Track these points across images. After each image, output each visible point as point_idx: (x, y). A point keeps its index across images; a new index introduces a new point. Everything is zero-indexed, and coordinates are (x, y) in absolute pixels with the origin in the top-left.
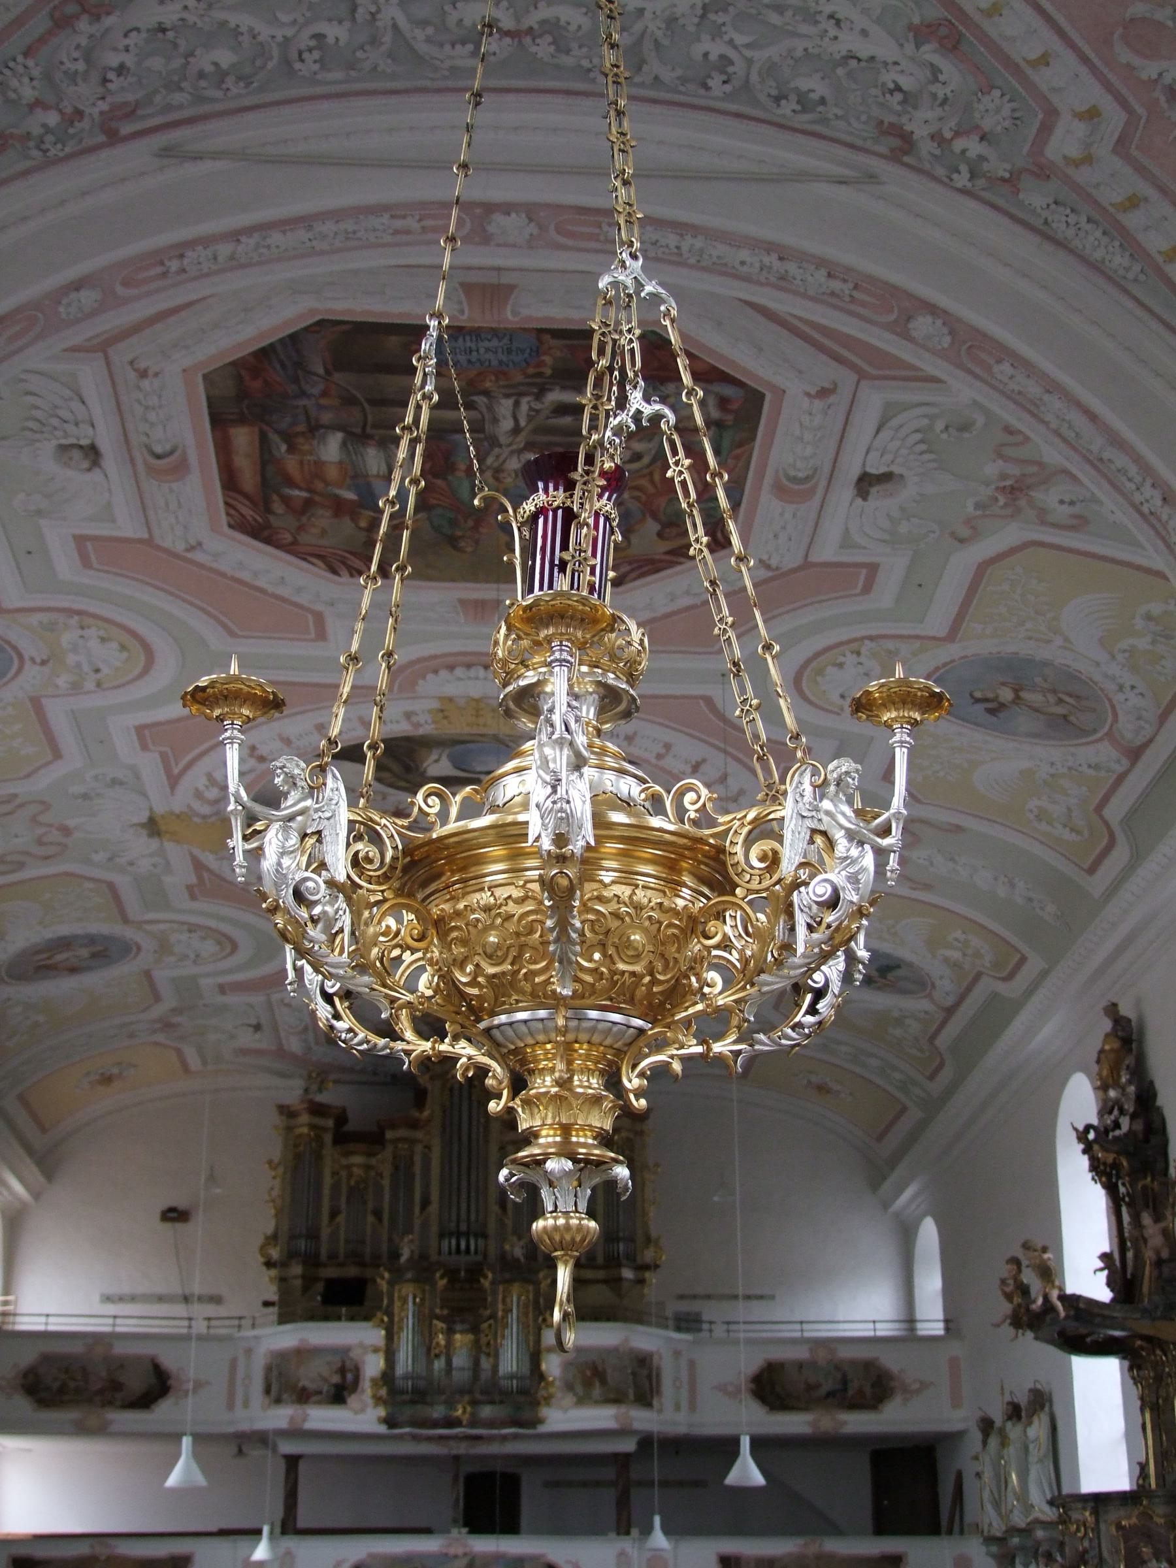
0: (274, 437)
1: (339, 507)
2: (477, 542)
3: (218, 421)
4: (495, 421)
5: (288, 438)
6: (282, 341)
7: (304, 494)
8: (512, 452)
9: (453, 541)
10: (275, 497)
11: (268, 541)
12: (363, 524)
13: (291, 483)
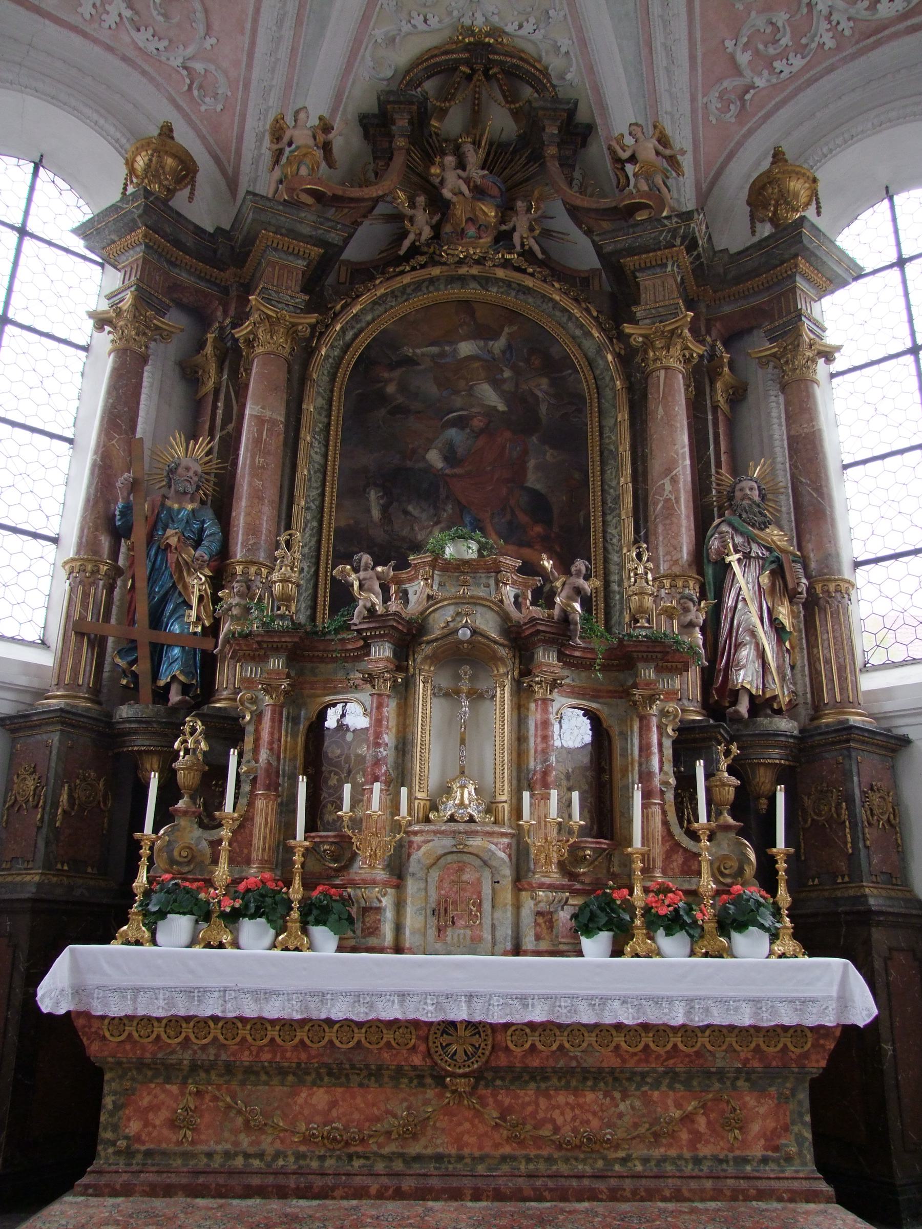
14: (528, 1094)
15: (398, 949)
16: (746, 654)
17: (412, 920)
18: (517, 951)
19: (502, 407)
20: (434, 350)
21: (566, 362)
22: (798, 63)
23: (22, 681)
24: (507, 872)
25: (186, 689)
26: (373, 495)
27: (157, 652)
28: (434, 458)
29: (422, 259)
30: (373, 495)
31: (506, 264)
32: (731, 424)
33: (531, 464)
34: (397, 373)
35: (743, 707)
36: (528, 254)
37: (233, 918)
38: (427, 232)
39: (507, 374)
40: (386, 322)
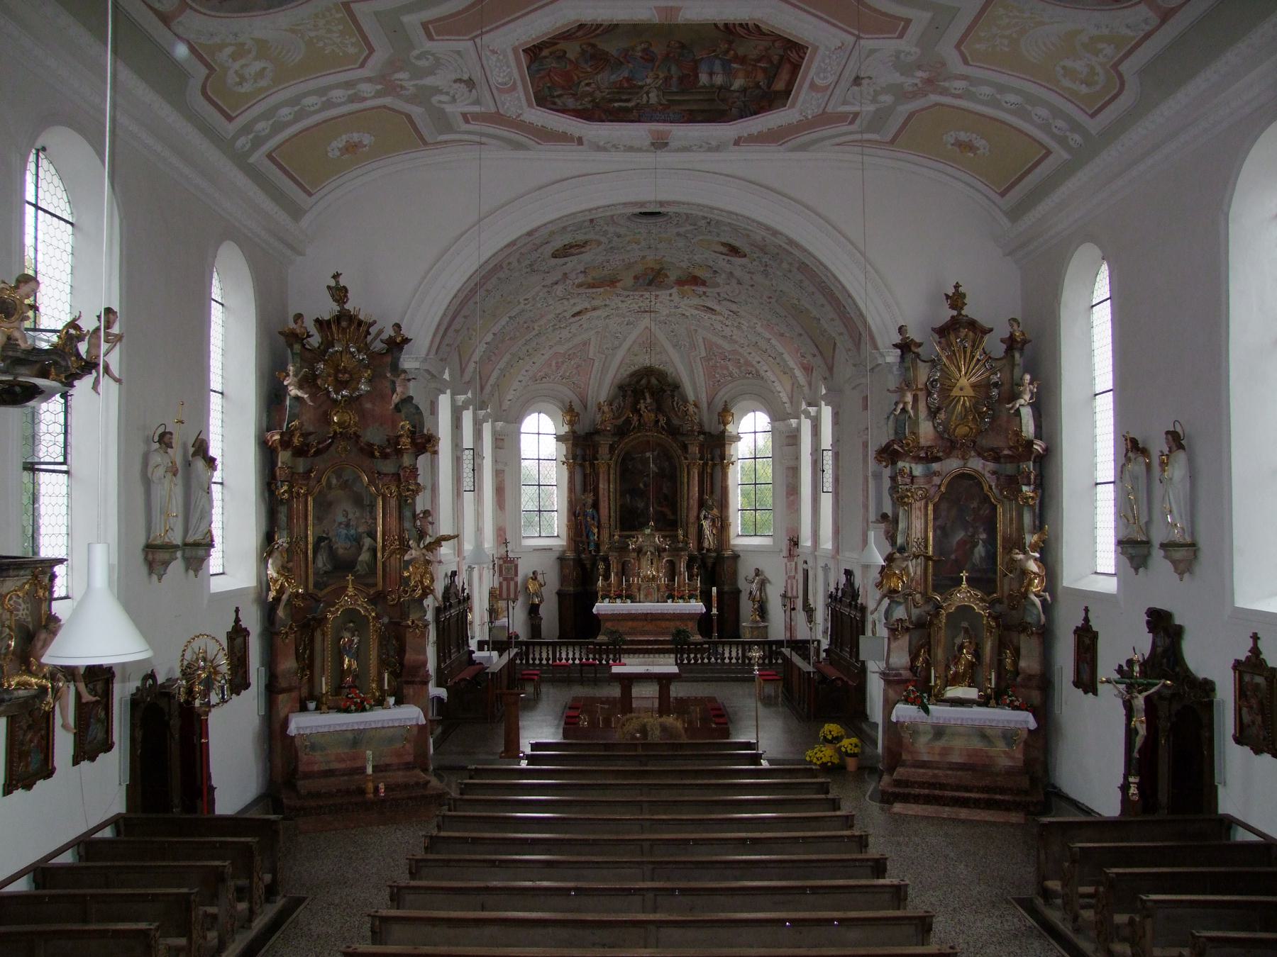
0: (764, 87)
1: (742, 60)
2: (668, 46)
3: (787, 93)
4: (658, 96)
5: (757, 86)
6: (746, 117)
7: (759, 64)
8: (649, 85)
9: (683, 46)
10: (775, 62)
11: (789, 41)
12: (732, 52)
13: (764, 70)
14: (659, 622)
15: (640, 602)
16: (706, 540)
17: (642, 596)
18: (658, 602)
23: (561, 549)
25: (595, 551)
26: (628, 496)
27: (588, 544)
28: (641, 485)
29: (635, 430)
30: (628, 496)
32: (712, 475)
35: (705, 551)
36: (662, 427)
37: (615, 599)
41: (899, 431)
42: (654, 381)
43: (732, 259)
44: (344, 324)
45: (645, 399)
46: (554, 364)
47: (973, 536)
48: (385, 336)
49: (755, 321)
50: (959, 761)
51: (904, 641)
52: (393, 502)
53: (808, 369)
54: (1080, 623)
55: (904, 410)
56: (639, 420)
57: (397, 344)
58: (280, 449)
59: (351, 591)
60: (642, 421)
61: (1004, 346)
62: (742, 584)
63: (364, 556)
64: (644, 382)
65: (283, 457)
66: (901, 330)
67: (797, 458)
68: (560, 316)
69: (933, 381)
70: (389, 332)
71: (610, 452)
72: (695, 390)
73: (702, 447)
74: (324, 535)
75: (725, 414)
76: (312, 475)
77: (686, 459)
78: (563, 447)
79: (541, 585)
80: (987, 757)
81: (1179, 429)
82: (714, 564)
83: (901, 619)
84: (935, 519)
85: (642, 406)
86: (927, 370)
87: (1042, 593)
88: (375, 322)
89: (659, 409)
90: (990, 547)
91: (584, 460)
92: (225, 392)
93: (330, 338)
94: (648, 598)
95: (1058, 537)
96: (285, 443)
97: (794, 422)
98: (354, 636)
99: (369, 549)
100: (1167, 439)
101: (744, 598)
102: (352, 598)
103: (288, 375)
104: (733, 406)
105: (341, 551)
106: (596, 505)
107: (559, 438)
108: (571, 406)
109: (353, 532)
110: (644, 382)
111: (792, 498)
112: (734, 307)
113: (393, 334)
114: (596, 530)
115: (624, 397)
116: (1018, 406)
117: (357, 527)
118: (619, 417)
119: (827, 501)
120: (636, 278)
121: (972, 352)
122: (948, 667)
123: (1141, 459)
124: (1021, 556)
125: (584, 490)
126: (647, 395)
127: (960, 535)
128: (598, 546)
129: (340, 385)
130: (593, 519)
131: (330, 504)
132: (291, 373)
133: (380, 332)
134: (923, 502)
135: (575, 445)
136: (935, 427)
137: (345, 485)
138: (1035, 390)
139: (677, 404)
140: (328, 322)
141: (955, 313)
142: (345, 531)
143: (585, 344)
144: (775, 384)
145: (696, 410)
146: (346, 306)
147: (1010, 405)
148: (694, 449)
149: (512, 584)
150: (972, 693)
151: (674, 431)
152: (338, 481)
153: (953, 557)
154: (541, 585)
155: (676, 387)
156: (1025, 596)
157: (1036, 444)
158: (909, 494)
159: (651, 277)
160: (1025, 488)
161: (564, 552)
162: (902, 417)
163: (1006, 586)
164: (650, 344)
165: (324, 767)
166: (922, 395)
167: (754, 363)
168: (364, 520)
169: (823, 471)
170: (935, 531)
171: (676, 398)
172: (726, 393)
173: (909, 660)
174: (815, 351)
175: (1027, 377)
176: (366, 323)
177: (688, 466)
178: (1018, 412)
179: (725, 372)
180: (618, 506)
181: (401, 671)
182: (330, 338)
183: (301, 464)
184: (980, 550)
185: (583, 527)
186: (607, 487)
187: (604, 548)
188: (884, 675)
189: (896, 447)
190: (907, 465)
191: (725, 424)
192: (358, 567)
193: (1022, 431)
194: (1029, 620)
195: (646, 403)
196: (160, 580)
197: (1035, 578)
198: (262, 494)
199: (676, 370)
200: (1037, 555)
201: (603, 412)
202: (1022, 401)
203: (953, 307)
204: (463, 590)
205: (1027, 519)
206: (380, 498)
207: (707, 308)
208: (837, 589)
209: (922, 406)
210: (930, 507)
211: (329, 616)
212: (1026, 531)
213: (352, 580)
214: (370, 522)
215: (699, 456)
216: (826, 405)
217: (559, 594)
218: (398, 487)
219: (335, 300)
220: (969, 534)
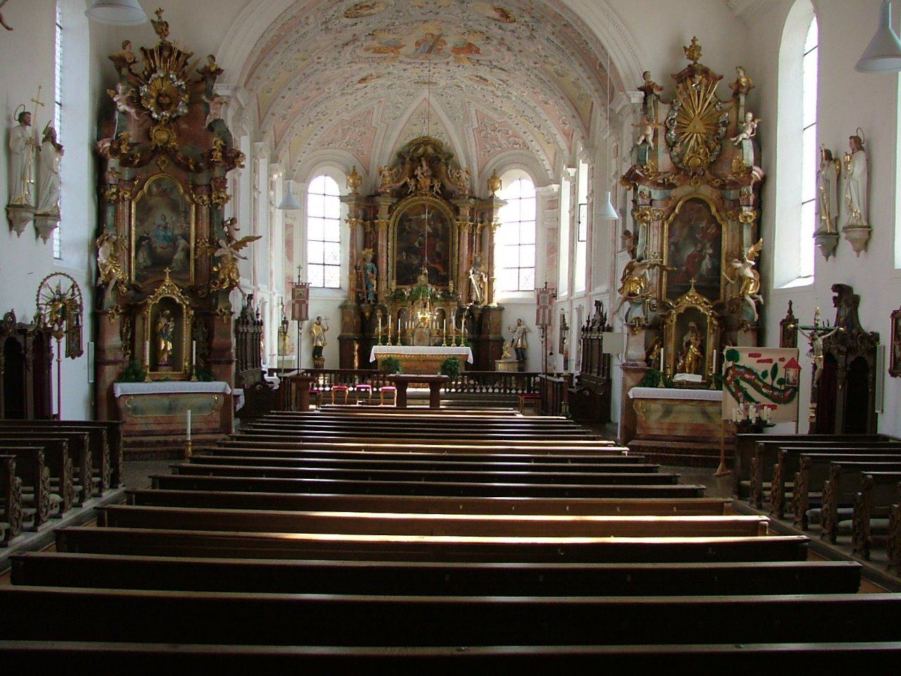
18: (430, 345)
19: (431, 231)
20: (416, 217)
21: (446, 219)
22: (500, 149)
24: (428, 335)
25: (373, 301)
27: (368, 294)
28: (417, 244)
29: (413, 194)
31: (432, 196)
32: (481, 236)
33: (437, 245)
34: (408, 223)
36: (437, 193)
38: (414, 188)
39: (432, 223)
40: (405, 210)
41: (641, 162)
42: (430, 150)
43: (504, 25)
44: (166, 53)
45: (421, 166)
46: (340, 131)
47: (701, 251)
48: (201, 66)
49: (522, 89)
50: (685, 435)
51: (641, 336)
52: (205, 210)
53: (568, 135)
54: (785, 315)
55: (645, 141)
56: (416, 185)
57: (211, 74)
58: (109, 156)
59: (168, 281)
60: (419, 186)
61: (732, 91)
62: (505, 334)
63: (179, 256)
64: (421, 151)
65: (113, 163)
66: (645, 75)
67: (558, 220)
68: (348, 81)
69: (671, 119)
70: (205, 62)
71: (389, 213)
72: (467, 158)
73: (472, 209)
74: (145, 235)
75: (492, 181)
76: (136, 183)
77: (458, 220)
78: (346, 207)
79: (324, 330)
80: (708, 431)
81: (860, 136)
82: (481, 316)
83: (638, 318)
84: (669, 237)
85: (418, 172)
86: (667, 111)
87: (756, 296)
88: (192, 54)
89: (435, 176)
90: (714, 260)
91: (365, 220)
92: (63, 103)
93: (153, 66)
94: (421, 342)
95: (772, 249)
96: (115, 152)
97: (555, 187)
98: (169, 321)
99: (183, 249)
100: (851, 143)
101: (507, 345)
102: (168, 288)
103: (117, 93)
104: (502, 174)
105: (159, 250)
106: (375, 260)
107: (342, 199)
108: (354, 170)
109: (169, 234)
110: (421, 151)
111: (551, 256)
112: (504, 76)
113: (208, 65)
114: (375, 282)
115: (403, 164)
116: (741, 139)
117: (173, 228)
118: (398, 181)
119: (581, 249)
120: (418, 44)
121: (704, 96)
122: (677, 361)
123: (832, 165)
124: (739, 265)
125: (365, 246)
126: (424, 163)
127: (690, 250)
128: (376, 296)
129: (161, 107)
130: (373, 272)
131: (150, 209)
132: (120, 91)
133: (197, 62)
134: (660, 221)
135: (357, 205)
136: (671, 158)
137: (164, 193)
138: (756, 126)
139: (451, 171)
140: (152, 52)
141: (692, 62)
142: (164, 233)
143: (369, 112)
144: (539, 153)
145: (467, 176)
146: (167, 39)
147: (735, 139)
148: (465, 212)
149: (304, 306)
150: (698, 378)
151: (446, 195)
152: (158, 188)
153: (684, 268)
154: (324, 330)
155: (450, 156)
156: (743, 300)
157: (755, 170)
158: (648, 212)
159: (431, 44)
160: (744, 208)
161: (346, 301)
162: (643, 147)
163: (728, 293)
164: (427, 115)
165: (144, 428)
166: (661, 129)
167: (521, 134)
168: (179, 224)
169: (579, 223)
170: (669, 247)
171: (449, 167)
172: (495, 163)
173: (644, 353)
174: (576, 114)
175: (750, 115)
176: (184, 54)
177: (459, 228)
178: (740, 145)
179: (495, 142)
180: (395, 262)
181: (210, 354)
182: (153, 66)
183: (127, 174)
184: (706, 264)
185: (364, 280)
186: (387, 245)
187: (381, 298)
188: (626, 369)
189: (637, 171)
190: (647, 189)
191: (494, 189)
192: (174, 264)
193: (743, 159)
194: (745, 318)
195: (423, 170)
196: (18, 235)
197: (751, 283)
198: (93, 196)
199: (450, 139)
200: (753, 263)
201: (384, 176)
202: (745, 135)
203: (690, 58)
204: (258, 315)
205: (747, 234)
206: (193, 207)
207: (481, 77)
208: (588, 322)
209: (661, 140)
210: (666, 226)
211: (150, 301)
212: (745, 245)
213: (169, 273)
214: (185, 225)
215: (469, 218)
216: (583, 163)
217: (340, 339)
218: (210, 196)
219: (158, 33)
220: (698, 249)
